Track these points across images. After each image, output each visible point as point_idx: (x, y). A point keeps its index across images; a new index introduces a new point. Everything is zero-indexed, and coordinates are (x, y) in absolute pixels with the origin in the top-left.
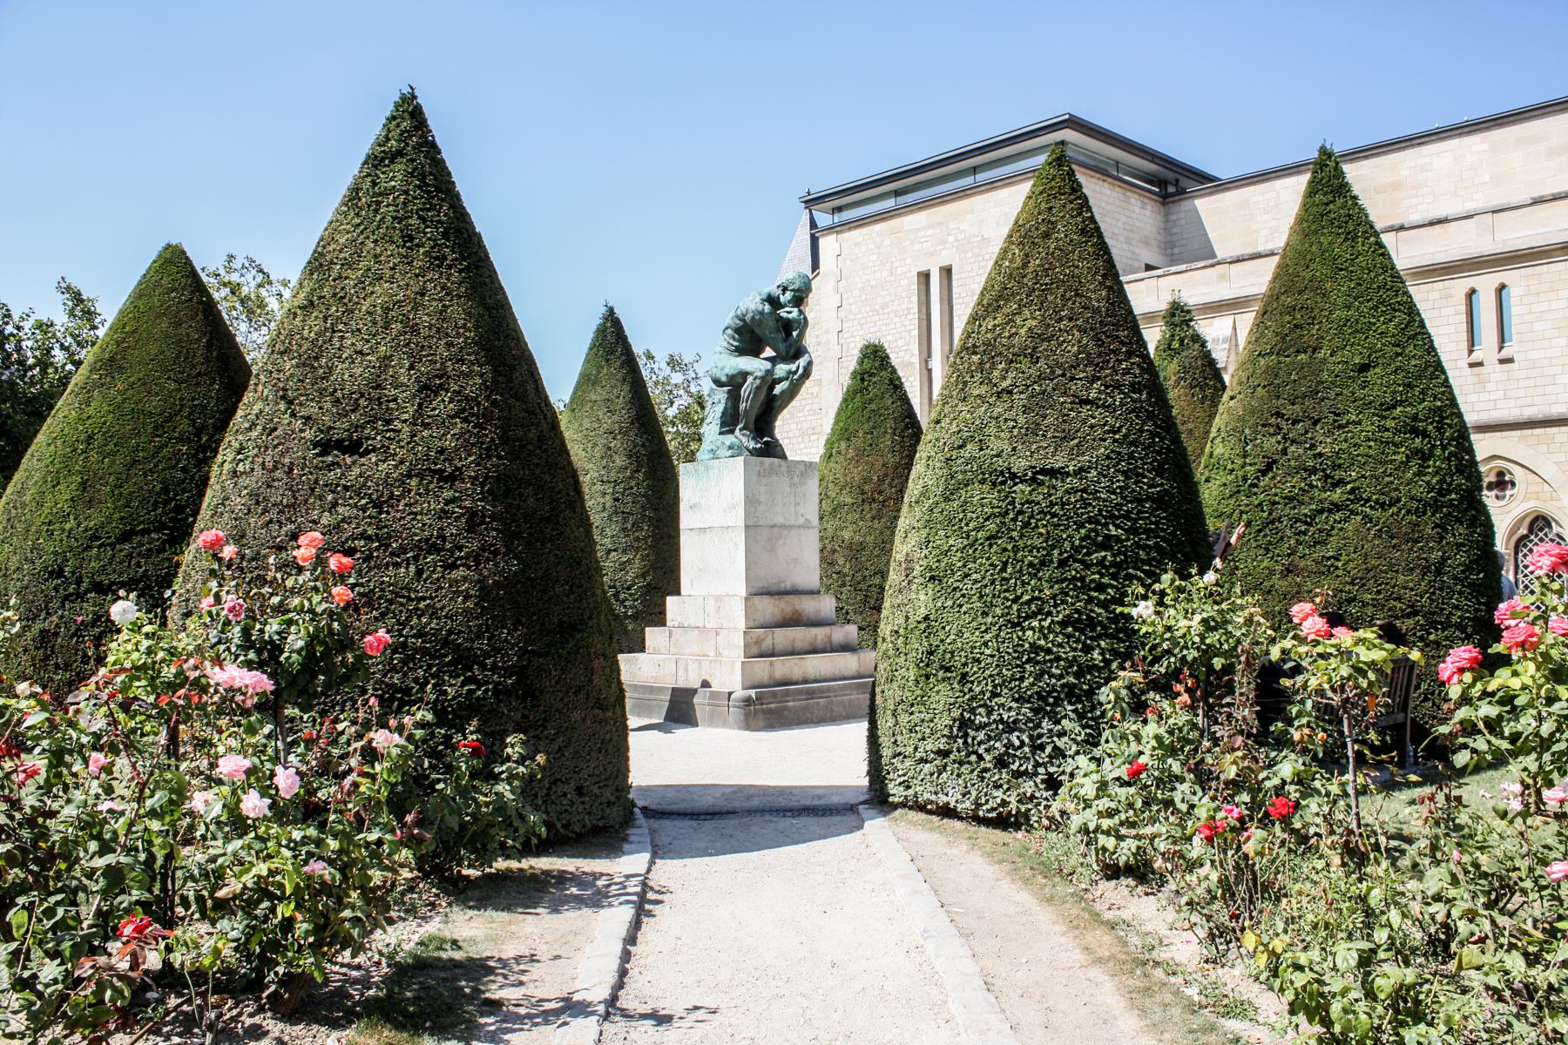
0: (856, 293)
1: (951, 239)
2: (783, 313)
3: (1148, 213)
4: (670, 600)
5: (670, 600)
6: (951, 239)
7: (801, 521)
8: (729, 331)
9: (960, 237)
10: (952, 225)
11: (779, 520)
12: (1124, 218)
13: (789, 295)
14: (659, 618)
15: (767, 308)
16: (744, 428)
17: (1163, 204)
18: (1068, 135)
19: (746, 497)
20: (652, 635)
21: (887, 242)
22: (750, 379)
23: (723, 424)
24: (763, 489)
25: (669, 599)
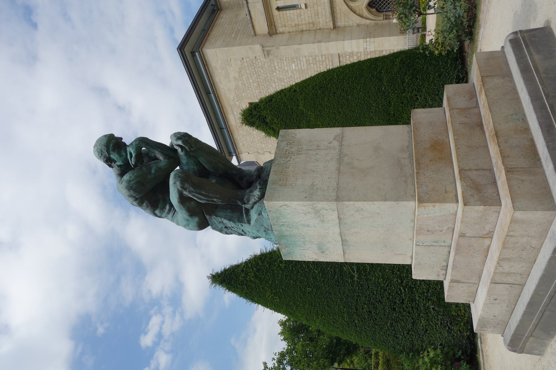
0: (263, 146)
1: (237, 103)
2: (132, 162)
3: (225, 16)
4: (417, 275)
5: (417, 275)
6: (237, 103)
7: (336, 144)
8: (157, 212)
9: (236, 99)
10: (232, 103)
11: (333, 165)
12: (226, 26)
13: (114, 156)
14: (437, 287)
15: (126, 177)
16: (242, 200)
17: (221, 10)
18: (187, 50)
19: (306, 199)
20: (451, 295)
21: (241, 132)
22: (186, 193)
23: (240, 221)
25: (414, 277)
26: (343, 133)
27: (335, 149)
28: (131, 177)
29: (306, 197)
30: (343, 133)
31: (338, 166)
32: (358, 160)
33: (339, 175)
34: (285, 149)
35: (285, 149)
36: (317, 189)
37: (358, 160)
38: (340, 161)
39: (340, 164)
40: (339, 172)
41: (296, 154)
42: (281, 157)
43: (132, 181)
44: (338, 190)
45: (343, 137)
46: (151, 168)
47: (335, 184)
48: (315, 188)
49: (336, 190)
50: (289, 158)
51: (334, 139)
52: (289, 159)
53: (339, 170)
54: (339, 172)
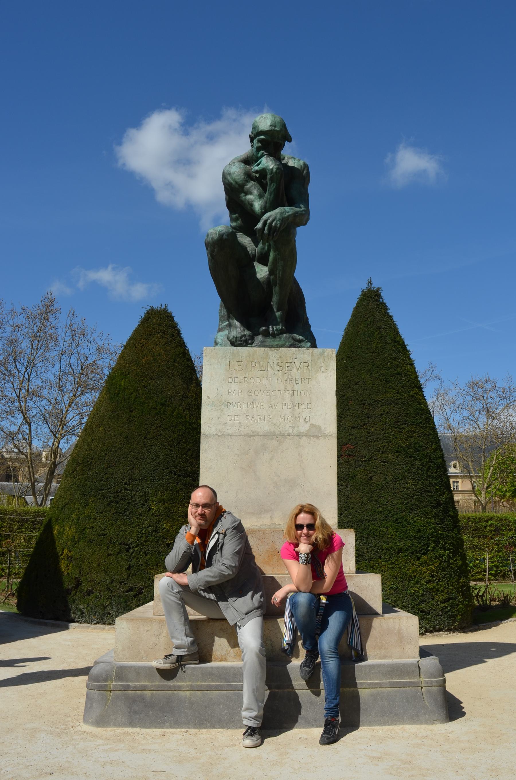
7: (304, 428)
11: (264, 426)
24: (234, 387)
26: (325, 436)
27: (294, 427)
28: (234, 173)
29: (208, 398)
30: (325, 436)
31: (261, 434)
32: (271, 459)
33: (244, 435)
34: (295, 361)
35: (295, 361)
36: (222, 410)
37: (271, 459)
38: (270, 436)
39: (265, 435)
40: (250, 436)
41: (286, 376)
42: (280, 357)
43: (231, 177)
44: (219, 436)
45: (317, 437)
46: (251, 193)
47: (230, 432)
48: (223, 407)
49: (219, 434)
50: (278, 368)
51: (312, 425)
52: (276, 368)
53: (254, 436)
54: (250, 436)
